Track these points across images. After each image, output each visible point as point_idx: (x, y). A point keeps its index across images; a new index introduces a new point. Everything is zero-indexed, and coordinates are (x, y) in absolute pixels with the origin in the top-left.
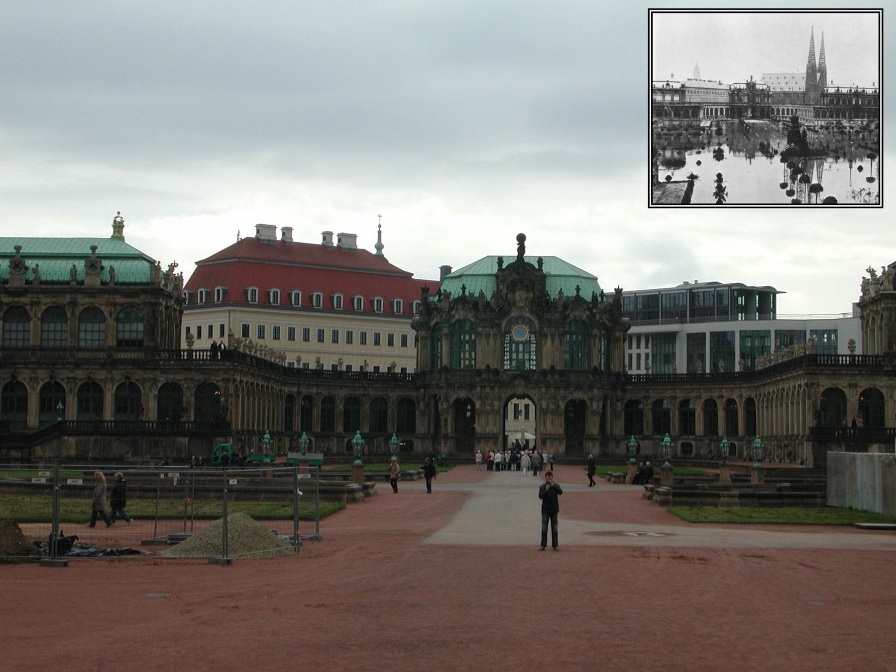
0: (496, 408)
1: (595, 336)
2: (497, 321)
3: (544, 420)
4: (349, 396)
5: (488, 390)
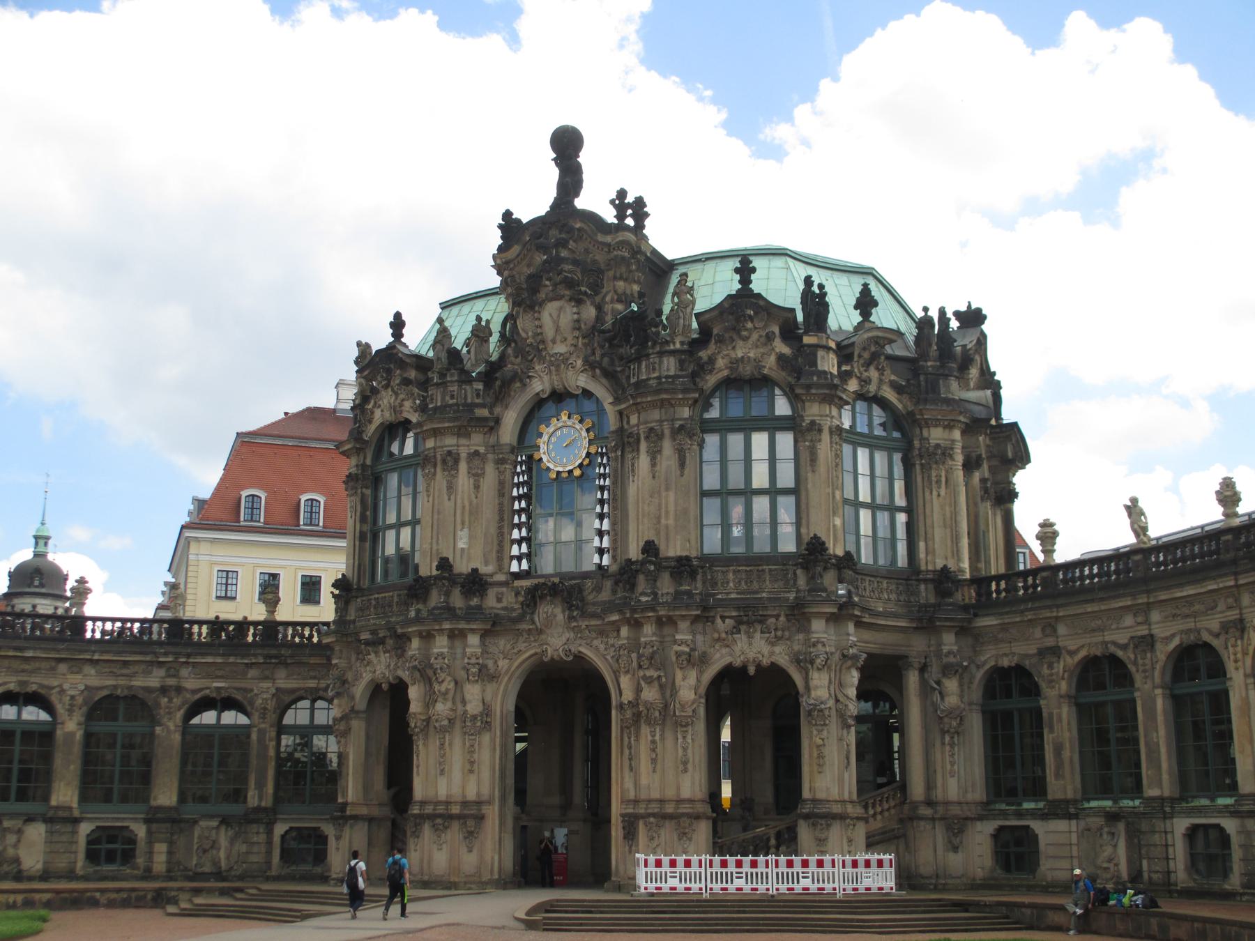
0: (474, 707)
2: (484, 412)
3: (630, 747)
4: (105, 693)
5: (441, 644)
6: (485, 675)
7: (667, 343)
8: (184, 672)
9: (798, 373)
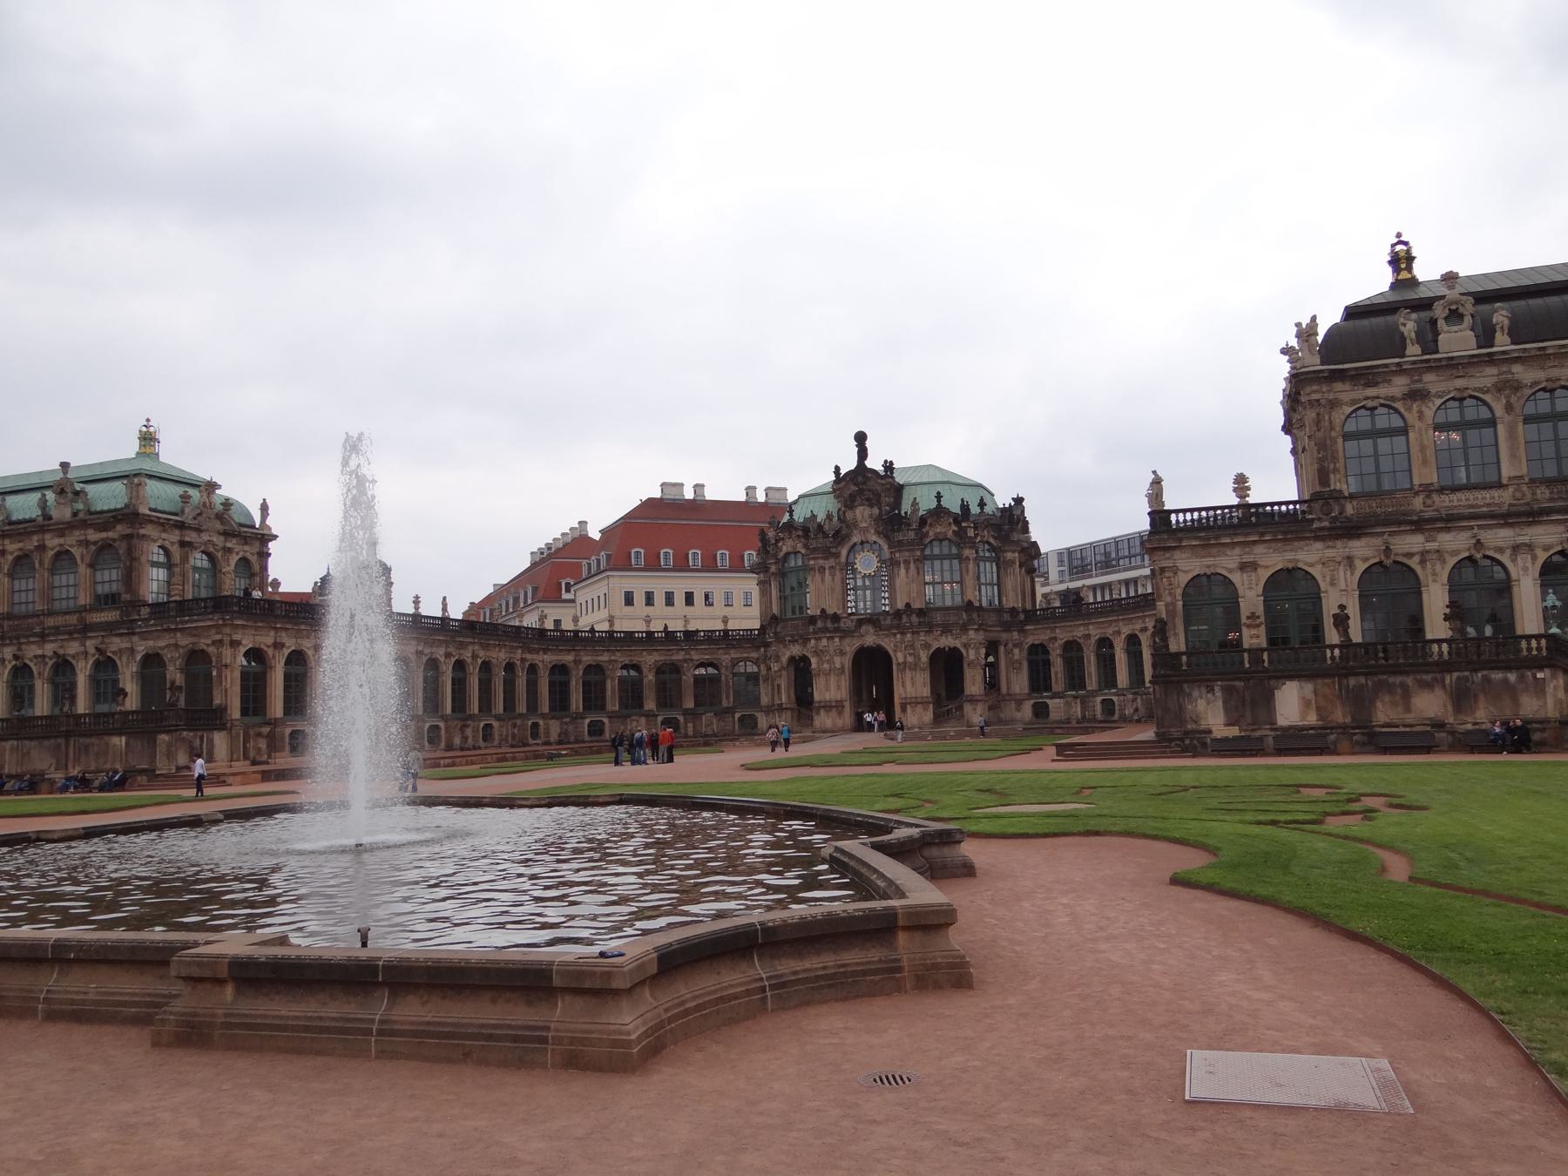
0: (838, 665)
1: (968, 558)
2: (834, 550)
5: (824, 642)
6: (842, 653)
7: (909, 525)
8: (692, 653)
9: (961, 538)
